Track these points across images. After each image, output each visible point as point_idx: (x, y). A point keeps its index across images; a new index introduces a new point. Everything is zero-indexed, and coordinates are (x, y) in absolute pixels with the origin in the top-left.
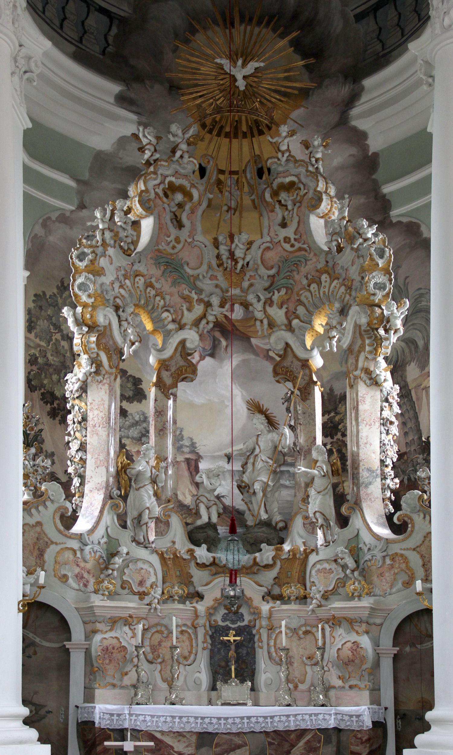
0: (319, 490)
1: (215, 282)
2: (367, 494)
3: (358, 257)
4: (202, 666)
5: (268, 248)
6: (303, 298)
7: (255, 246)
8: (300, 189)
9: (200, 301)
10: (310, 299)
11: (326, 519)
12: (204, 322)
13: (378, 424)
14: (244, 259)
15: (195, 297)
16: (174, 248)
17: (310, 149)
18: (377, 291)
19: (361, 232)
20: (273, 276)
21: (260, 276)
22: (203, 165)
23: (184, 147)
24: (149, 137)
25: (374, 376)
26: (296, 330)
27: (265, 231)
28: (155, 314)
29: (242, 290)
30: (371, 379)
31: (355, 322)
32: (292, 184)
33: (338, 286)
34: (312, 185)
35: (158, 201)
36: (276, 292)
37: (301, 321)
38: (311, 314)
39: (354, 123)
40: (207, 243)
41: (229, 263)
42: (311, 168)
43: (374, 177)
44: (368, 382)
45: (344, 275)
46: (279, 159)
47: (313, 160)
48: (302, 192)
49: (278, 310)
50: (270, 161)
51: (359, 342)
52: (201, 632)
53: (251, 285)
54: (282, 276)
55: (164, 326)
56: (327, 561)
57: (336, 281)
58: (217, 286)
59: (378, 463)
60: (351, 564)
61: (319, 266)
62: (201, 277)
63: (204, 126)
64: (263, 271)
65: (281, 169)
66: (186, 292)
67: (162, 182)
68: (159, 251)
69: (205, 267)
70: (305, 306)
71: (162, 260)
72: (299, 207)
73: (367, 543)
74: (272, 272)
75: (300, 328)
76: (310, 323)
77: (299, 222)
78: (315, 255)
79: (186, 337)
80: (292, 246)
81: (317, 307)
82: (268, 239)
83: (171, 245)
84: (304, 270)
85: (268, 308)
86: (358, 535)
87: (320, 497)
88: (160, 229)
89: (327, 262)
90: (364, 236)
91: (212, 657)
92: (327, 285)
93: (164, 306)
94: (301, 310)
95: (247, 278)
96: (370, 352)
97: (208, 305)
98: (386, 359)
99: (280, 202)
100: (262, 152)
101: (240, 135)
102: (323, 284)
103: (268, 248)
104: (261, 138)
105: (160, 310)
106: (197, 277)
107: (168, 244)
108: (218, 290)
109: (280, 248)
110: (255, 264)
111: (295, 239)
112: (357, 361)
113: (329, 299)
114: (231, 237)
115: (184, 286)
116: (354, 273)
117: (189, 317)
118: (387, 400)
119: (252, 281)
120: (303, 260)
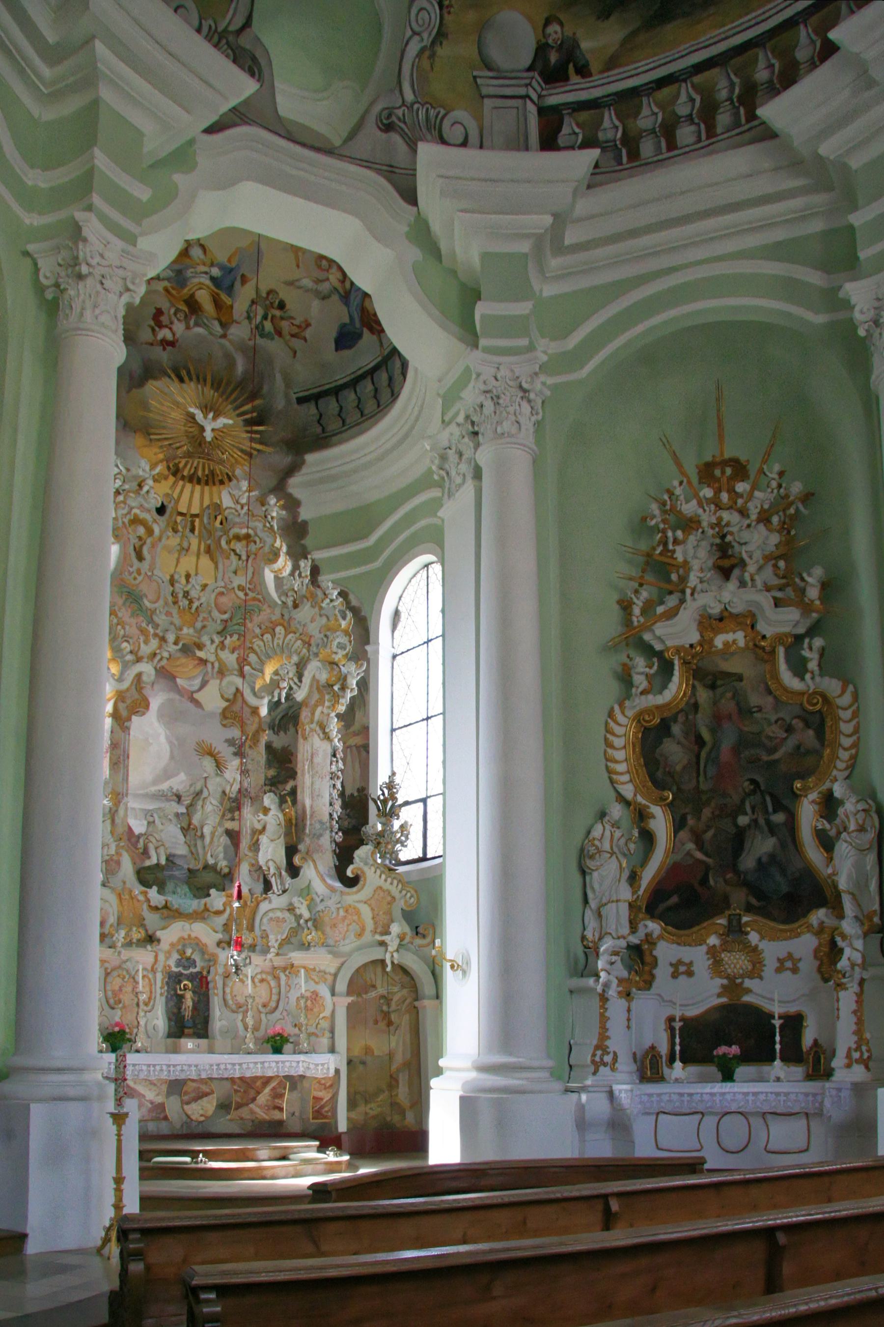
0: (273, 838)
1: (169, 618)
2: (319, 846)
3: (321, 615)
4: (160, 1013)
5: (222, 594)
6: (256, 647)
7: (208, 589)
8: (255, 542)
9: (156, 635)
10: (263, 648)
11: (278, 868)
12: (158, 657)
13: (328, 778)
14: (199, 599)
15: (152, 631)
16: (135, 579)
17: (267, 507)
18: (340, 651)
19: (327, 592)
20: (226, 621)
21: (213, 620)
22: (165, 503)
23: (150, 482)
24: (121, 468)
25: (327, 730)
26: (247, 677)
27: (220, 575)
28: (116, 643)
29: (196, 631)
30: (324, 733)
31: (314, 676)
32: (247, 537)
33: (293, 640)
34: (269, 541)
35: (125, 531)
36: (228, 637)
37: (253, 669)
38: (263, 663)
39: (290, 490)
40: (165, 580)
41: (184, 603)
42: (268, 525)
43: (303, 542)
44: (321, 735)
45: (301, 631)
46: (237, 511)
47: (269, 517)
48: (259, 545)
49: (230, 655)
50: (227, 512)
51: (316, 696)
52: (159, 976)
53: (204, 627)
54: (234, 621)
55: (123, 656)
56: (281, 910)
57: (292, 635)
58: (172, 623)
59: (328, 817)
60: (306, 915)
61: (274, 618)
62: (158, 612)
63: (169, 468)
64: (216, 614)
65: (237, 520)
66: (144, 625)
67: (129, 513)
68: (122, 580)
69: (161, 602)
70: (257, 654)
71: (125, 590)
72: (254, 559)
73: (319, 893)
74: (226, 617)
75: (251, 675)
76: (262, 671)
77: (253, 573)
78: (269, 606)
79: (143, 670)
80: (246, 594)
81: (269, 657)
82: (223, 584)
83: (133, 576)
84: (257, 619)
85: (219, 651)
86: (309, 886)
87: (273, 845)
88: (125, 558)
89: (283, 615)
90: (330, 596)
91: (167, 1003)
92: (282, 636)
93: (124, 636)
94: (252, 658)
95: (200, 619)
96: (329, 707)
97: (163, 639)
98: (338, 716)
99: (234, 551)
100: (221, 502)
101: (195, 480)
102: (277, 636)
103: (222, 594)
104: (222, 487)
105: (120, 639)
106: (153, 612)
107: (130, 573)
108: (172, 627)
109: (234, 595)
110: (208, 605)
111: (249, 589)
112: (313, 714)
113: (284, 649)
114: (188, 576)
115: (142, 618)
116: (314, 629)
117: (146, 650)
118: (334, 755)
119: (205, 623)
120: (257, 610)
